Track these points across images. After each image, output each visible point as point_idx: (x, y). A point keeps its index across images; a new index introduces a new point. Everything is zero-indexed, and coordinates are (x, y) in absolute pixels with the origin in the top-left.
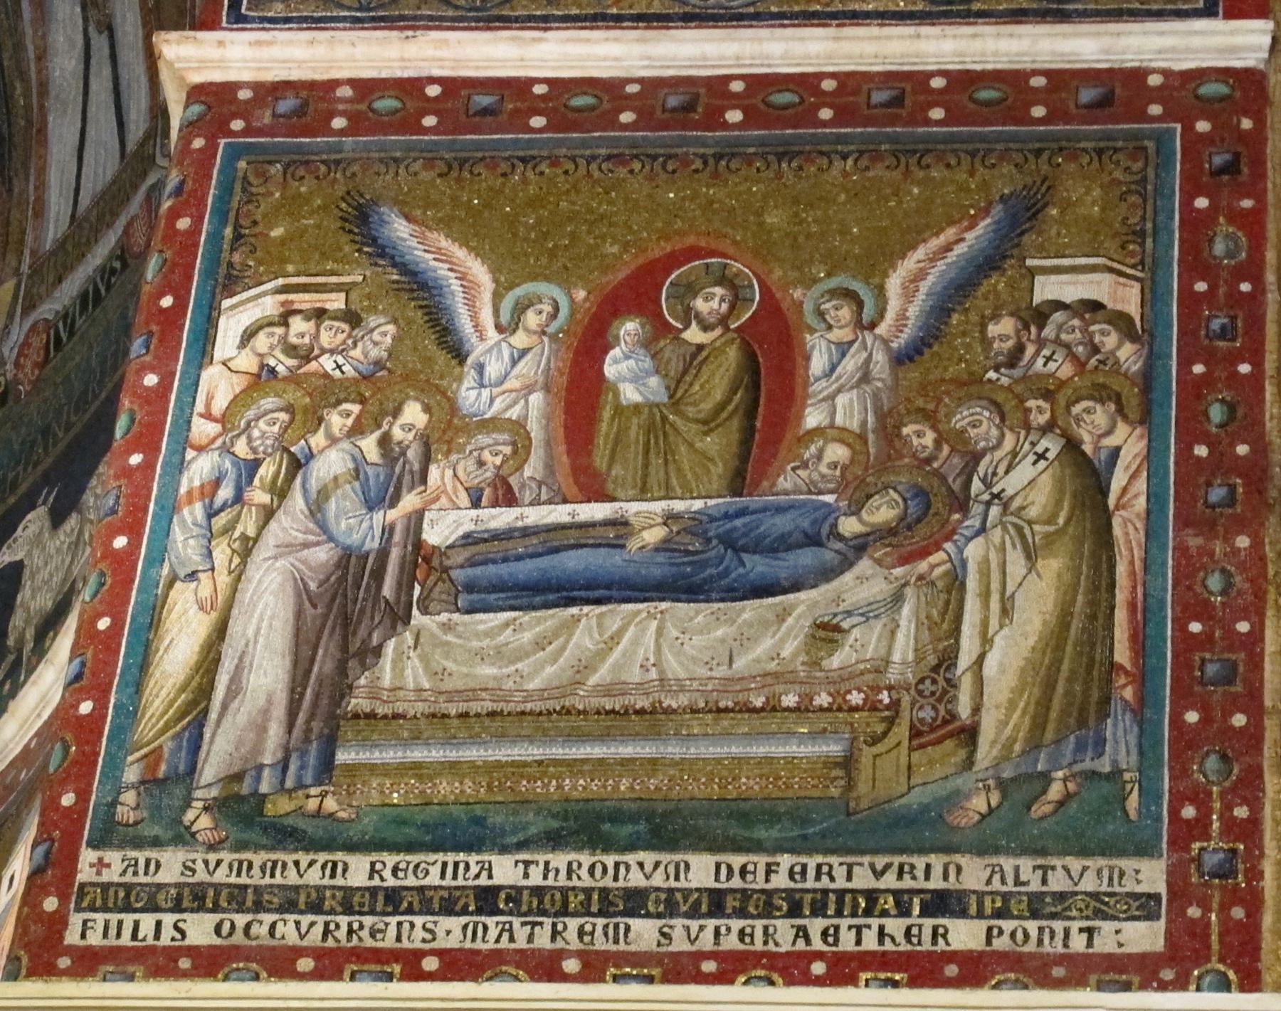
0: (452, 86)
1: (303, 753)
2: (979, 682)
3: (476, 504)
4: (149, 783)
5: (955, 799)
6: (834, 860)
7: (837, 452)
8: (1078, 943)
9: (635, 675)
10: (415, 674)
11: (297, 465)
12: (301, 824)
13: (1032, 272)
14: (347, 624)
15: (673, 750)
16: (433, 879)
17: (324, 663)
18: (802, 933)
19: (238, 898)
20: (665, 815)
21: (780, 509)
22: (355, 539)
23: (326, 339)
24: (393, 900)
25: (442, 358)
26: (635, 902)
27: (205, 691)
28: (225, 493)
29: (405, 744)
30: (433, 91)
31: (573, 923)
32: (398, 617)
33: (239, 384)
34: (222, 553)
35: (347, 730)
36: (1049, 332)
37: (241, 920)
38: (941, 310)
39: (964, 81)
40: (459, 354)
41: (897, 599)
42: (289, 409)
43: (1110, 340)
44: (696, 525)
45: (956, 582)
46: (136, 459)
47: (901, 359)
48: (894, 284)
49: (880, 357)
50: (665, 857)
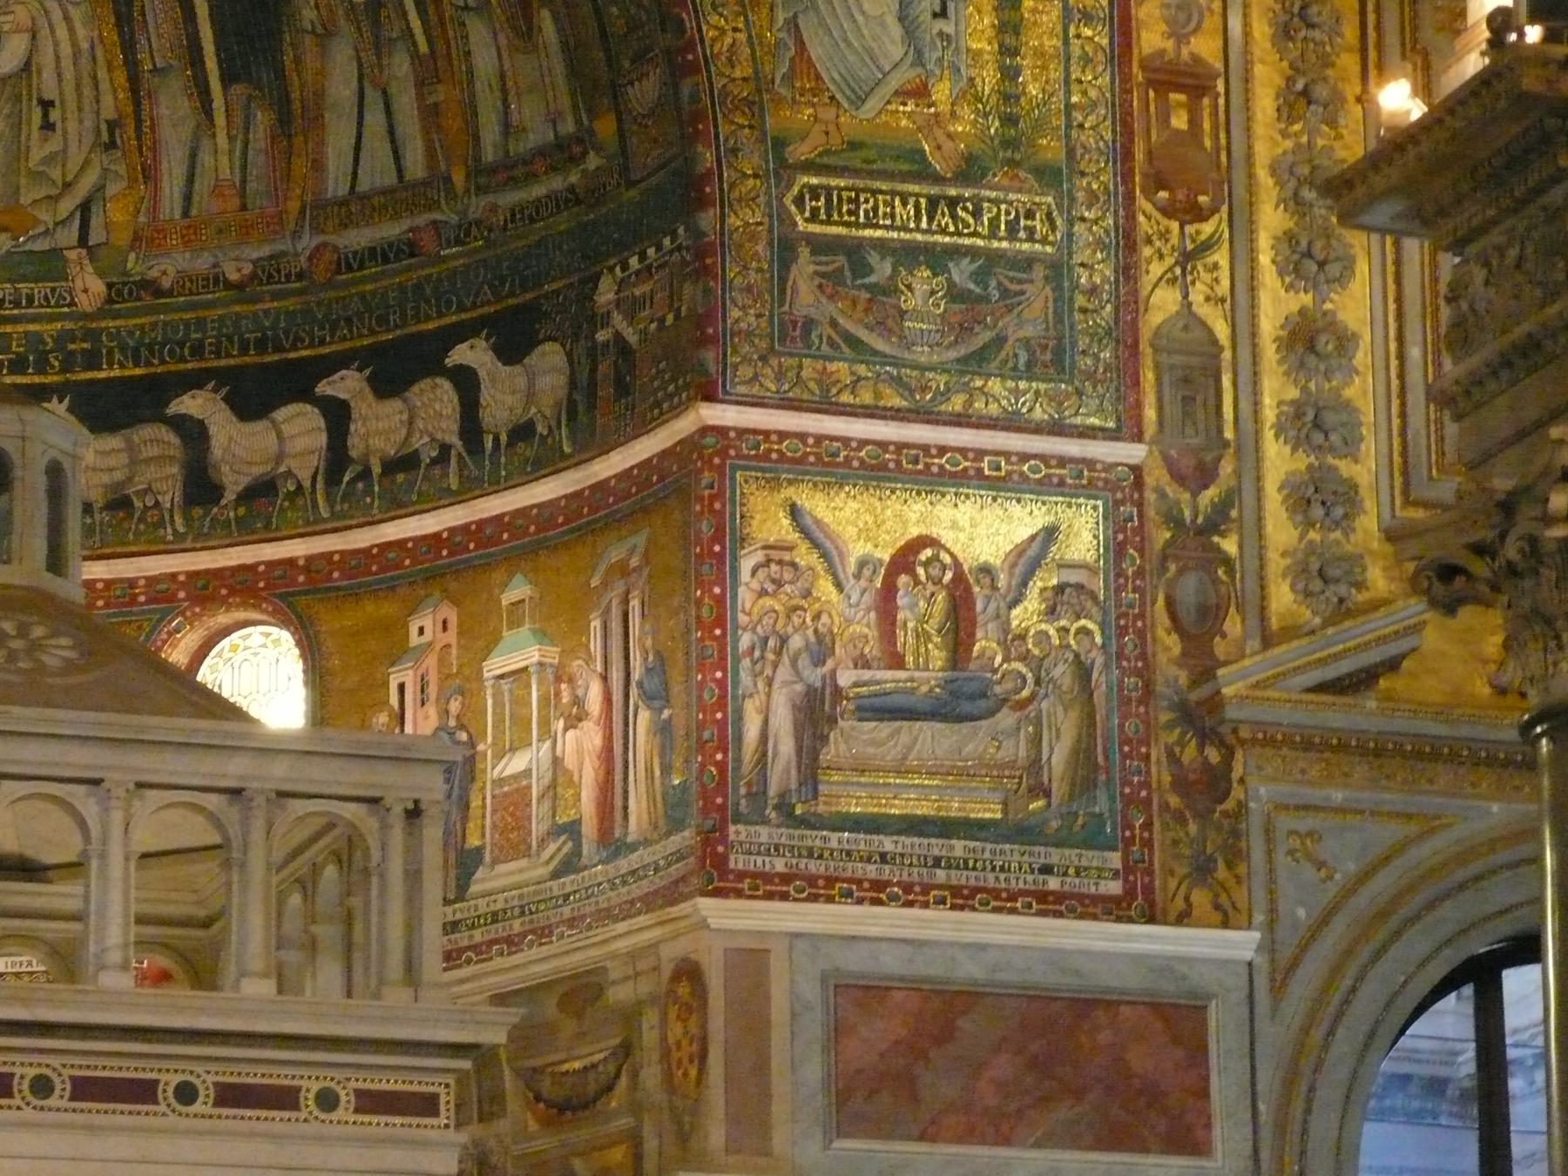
2: (1050, 769)
3: (856, 667)
5: (1046, 822)
8: (1093, 889)
11: (784, 640)
14: (814, 723)
16: (862, 846)
17: (807, 742)
18: (997, 879)
21: (971, 679)
22: (811, 680)
26: (937, 862)
27: (765, 754)
28: (757, 654)
32: (833, 721)
34: (761, 685)
36: (1065, 597)
37: (794, 861)
43: (1089, 604)
45: (1039, 718)
49: (1002, 604)
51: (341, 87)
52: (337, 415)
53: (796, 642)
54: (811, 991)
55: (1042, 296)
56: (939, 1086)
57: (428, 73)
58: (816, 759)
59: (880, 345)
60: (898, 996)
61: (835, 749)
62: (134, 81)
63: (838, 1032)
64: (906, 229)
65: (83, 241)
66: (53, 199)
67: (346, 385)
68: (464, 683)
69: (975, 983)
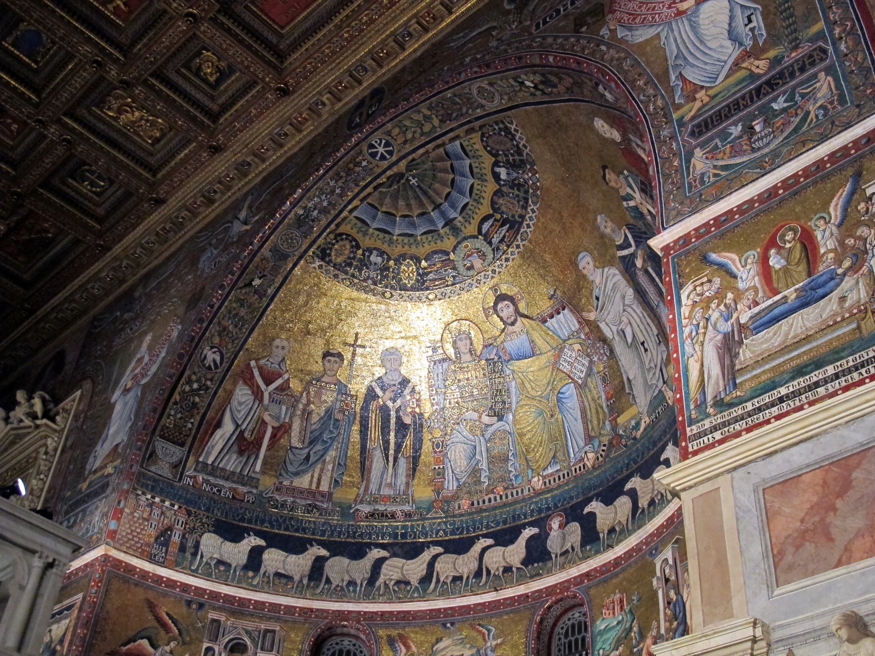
0: (715, 219)
1: (729, 384)
3: (750, 309)
4: (697, 406)
6: (863, 353)
7: (831, 255)
9: (799, 331)
10: (748, 355)
12: (733, 401)
13: (864, 190)
14: (730, 350)
15: (815, 344)
16: (767, 400)
17: (727, 362)
18: (861, 374)
19: (724, 424)
20: (818, 360)
21: (822, 275)
23: (705, 289)
24: (760, 409)
25: (732, 280)
26: (817, 385)
27: (703, 381)
29: (751, 371)
30: (712, 222)
31: (803, 396)
32: (741, 343)
33: (689, 308)
34: (697, 347)
35: (737, 375)
37: (726, 429)
38: (845, 209)
39: (832, 155)
40: (735, 277)
41: (857, 282)
42: (702, 308)
44: (803, 289)
46: (673, 336)
47: (839, 226)
48: (831, 210)
50: (820, 371)
53: (715, 315)
54: (748, 500)
55: (826, 84)
58: (733, 365)
59: (738, 160)
60: (806, 478)
61: (745, 355)
62: (655, 315)
64: (746, 106)
65: (664, 382)
66: (654, 374)
69: (862, 445)
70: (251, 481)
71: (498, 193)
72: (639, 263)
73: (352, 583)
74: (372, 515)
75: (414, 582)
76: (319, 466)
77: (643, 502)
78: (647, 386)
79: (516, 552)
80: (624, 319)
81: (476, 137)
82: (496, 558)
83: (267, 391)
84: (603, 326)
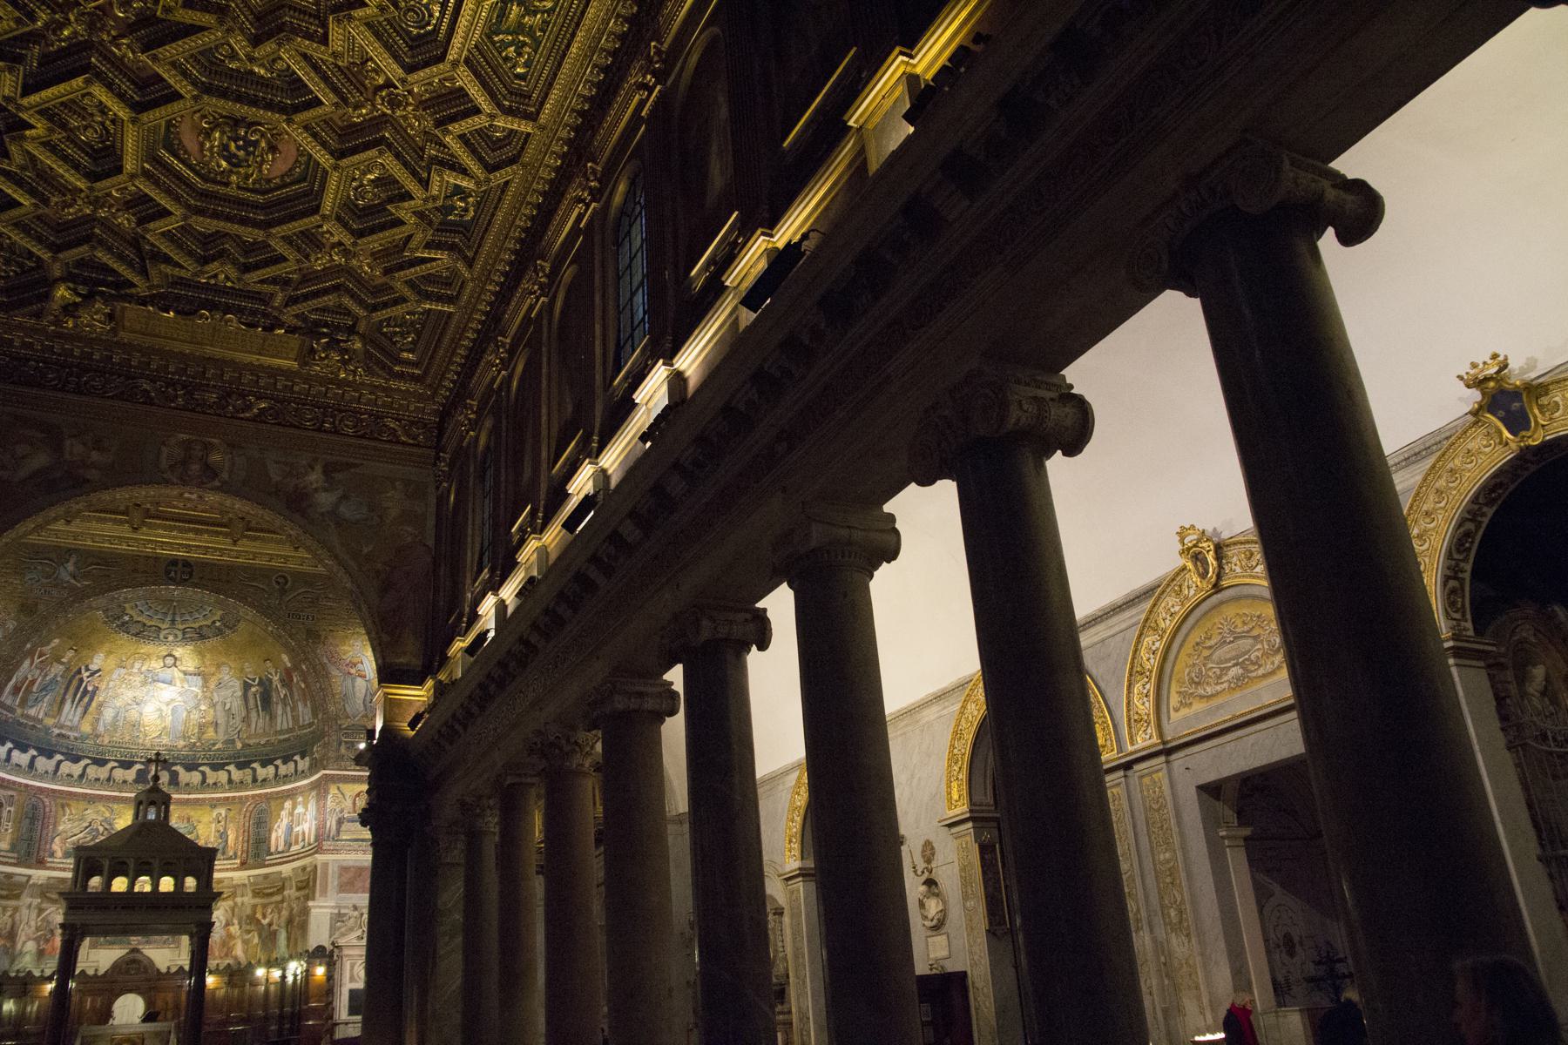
51: (280, 712)
52: (277, 767)
54: (336, 869)
56: (359, 884)
57: (294, 709)
61: (344, 827)
63: (340, 875)
67: (278, 762)
68: (291, 814)
70: (11, 709)
71: (209, 626)
72: (253, 689)
73: (46, 772)
74: (59, 735)
75: (76, 776)
76: (40, 705)
77: (210, 781)
78: (226, 732)
79: (130, 775)
80: (229, 700)
81: (221, 612)
82: (119, 774)
83: (37, 661)
84: (215, 694)
